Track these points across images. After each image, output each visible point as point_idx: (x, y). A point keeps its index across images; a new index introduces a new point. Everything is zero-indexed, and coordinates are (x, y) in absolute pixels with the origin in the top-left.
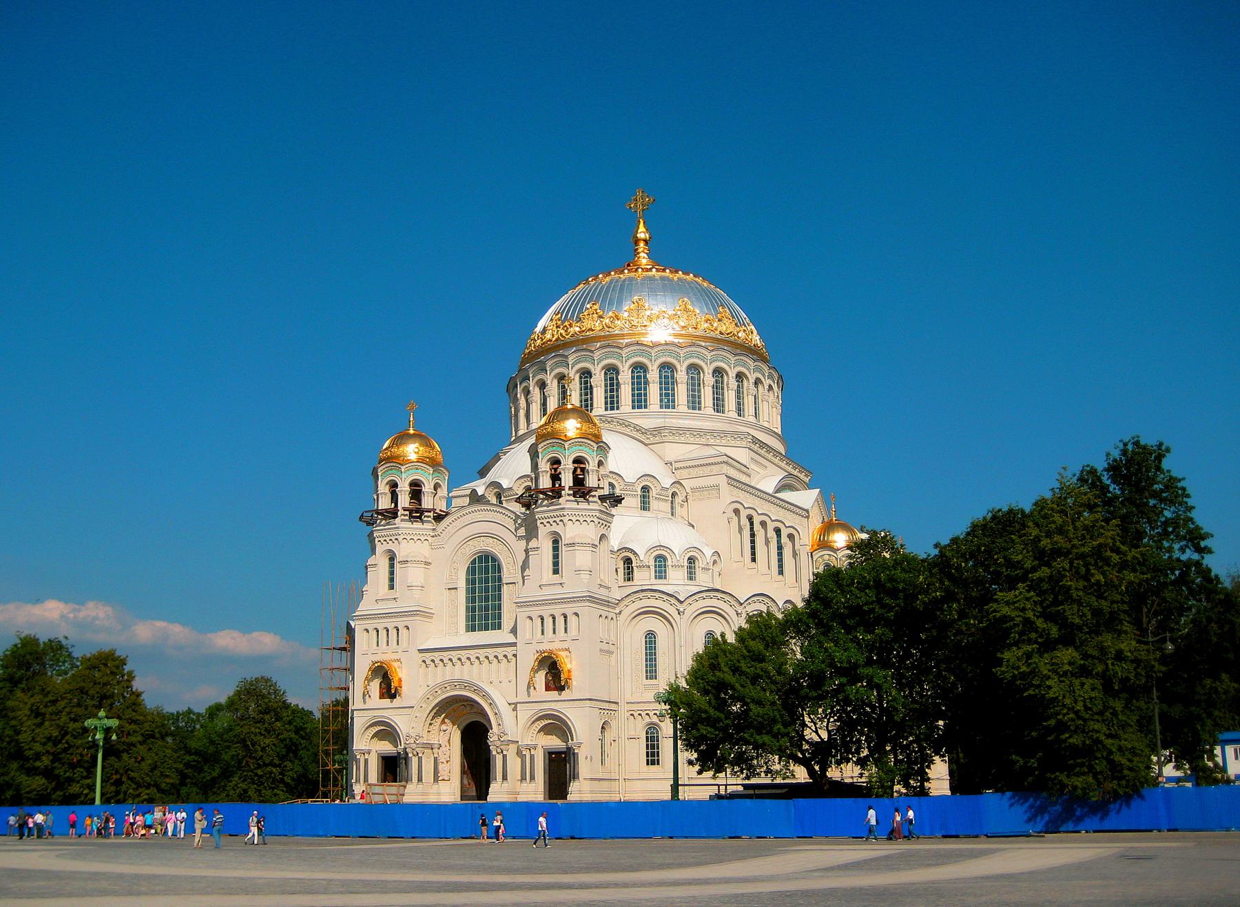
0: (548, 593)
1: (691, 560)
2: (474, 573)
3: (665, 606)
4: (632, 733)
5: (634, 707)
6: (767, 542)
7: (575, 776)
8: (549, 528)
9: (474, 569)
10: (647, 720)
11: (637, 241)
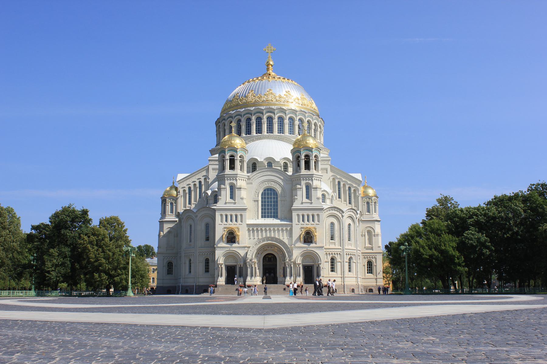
1: (332, 196)
2: (265, 195)
3: (338, 213)
4: (326, 260)
5: (327, 250)
6: (344, 190)
7: (318, 275)
8: (305, 182)
9: (265, 193)
10: (331, 255)
11: (268, 65)
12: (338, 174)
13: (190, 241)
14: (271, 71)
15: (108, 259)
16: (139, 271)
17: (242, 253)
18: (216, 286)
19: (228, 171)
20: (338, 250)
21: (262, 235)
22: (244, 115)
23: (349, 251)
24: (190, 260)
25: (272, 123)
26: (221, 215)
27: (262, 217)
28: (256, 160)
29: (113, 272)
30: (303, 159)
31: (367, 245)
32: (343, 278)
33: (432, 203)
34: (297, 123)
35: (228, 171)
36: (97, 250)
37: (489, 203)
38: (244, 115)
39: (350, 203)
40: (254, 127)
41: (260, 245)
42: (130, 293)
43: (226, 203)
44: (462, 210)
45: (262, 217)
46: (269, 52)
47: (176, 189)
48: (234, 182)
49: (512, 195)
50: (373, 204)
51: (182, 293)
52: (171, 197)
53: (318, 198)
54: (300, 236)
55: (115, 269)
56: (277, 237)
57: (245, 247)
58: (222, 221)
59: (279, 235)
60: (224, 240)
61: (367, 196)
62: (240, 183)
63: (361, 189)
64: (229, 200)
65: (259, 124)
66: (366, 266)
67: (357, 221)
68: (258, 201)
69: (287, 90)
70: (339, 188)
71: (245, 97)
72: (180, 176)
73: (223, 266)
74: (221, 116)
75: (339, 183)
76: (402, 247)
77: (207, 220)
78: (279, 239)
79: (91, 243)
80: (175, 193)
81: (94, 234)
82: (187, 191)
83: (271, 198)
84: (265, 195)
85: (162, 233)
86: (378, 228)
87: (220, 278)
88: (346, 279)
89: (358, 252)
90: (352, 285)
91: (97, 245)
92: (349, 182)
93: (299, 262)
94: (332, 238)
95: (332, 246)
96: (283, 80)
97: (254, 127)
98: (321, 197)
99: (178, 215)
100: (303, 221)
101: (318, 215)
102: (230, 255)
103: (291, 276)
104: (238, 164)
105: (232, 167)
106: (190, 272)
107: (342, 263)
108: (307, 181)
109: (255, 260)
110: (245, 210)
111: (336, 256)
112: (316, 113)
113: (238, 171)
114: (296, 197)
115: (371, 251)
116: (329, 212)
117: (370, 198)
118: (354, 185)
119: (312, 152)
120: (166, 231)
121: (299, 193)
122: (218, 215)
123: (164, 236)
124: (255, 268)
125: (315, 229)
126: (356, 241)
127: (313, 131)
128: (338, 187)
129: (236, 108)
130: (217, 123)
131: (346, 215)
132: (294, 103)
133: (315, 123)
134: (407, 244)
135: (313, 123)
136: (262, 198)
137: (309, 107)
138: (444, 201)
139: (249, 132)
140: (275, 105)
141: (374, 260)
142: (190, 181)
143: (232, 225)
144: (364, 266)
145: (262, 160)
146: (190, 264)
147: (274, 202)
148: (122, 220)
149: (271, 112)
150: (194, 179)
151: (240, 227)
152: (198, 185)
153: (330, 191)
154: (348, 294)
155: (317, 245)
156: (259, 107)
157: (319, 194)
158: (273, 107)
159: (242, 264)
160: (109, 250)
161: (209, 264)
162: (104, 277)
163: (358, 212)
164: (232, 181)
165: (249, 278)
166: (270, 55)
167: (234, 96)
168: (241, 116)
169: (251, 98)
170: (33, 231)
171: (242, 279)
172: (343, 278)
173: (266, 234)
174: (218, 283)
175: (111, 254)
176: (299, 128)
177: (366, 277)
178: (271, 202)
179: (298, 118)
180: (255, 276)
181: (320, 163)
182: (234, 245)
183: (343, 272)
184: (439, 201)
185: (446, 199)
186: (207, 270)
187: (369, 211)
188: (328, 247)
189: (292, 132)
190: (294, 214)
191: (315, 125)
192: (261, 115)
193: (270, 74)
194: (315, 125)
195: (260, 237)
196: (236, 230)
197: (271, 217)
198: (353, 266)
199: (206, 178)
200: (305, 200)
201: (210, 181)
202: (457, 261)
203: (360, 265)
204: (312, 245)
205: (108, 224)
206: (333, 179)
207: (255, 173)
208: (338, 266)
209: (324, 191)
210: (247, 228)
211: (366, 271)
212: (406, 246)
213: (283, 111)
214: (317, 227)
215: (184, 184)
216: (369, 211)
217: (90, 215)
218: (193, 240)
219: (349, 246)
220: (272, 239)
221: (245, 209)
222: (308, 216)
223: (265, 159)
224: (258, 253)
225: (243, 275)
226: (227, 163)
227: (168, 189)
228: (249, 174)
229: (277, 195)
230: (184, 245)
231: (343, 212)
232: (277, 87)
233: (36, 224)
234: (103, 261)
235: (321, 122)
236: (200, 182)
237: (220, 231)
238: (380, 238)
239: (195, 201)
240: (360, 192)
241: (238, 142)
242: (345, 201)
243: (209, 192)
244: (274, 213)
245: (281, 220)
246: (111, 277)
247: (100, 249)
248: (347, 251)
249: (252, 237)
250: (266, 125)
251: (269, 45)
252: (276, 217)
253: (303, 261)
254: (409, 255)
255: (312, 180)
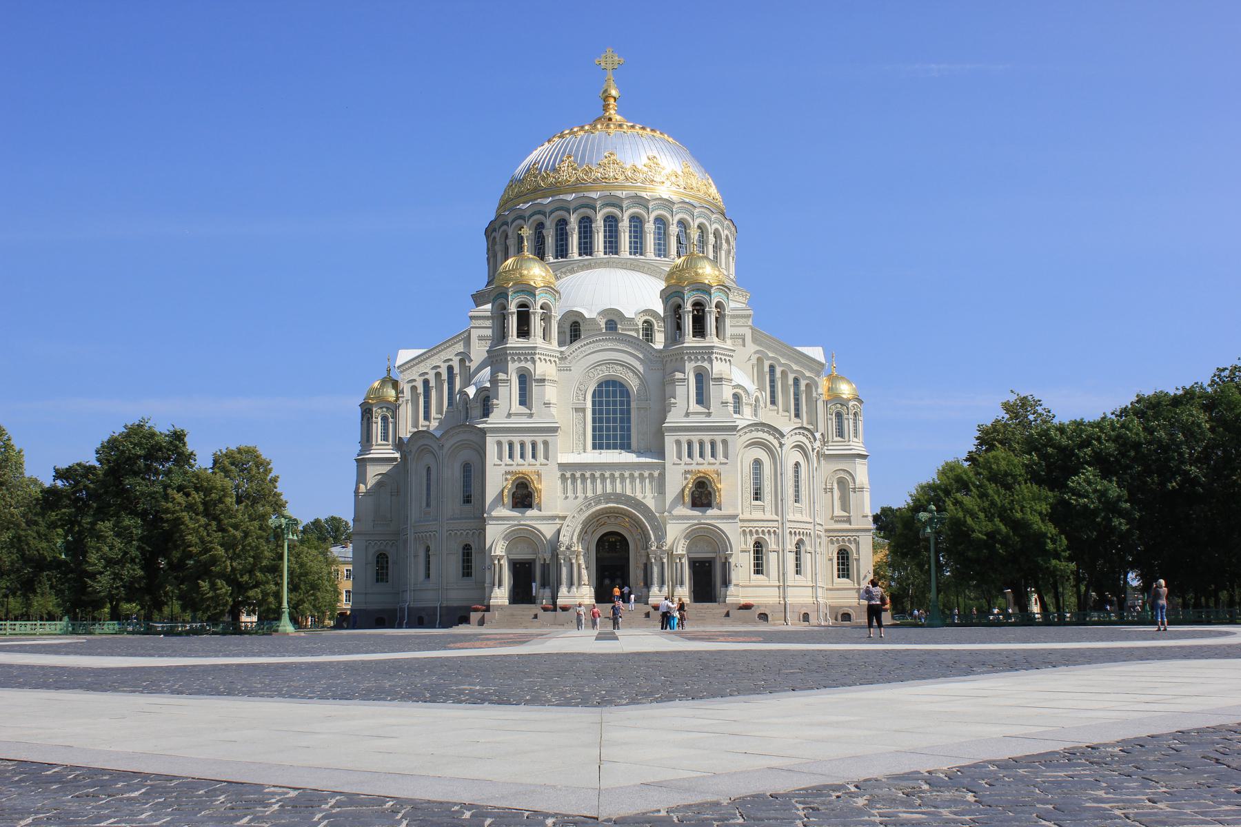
0: (694, 421)
1: (757, 400)
2: (600, 396)
3: (771, 438)
4: (743, 546)
5: (746, 524)
6: (785, 386)
7: (726, 583)
8: (693, 364)
9: (600, 393)
10: (755, 536)
11: (606, 98)
12: (769, 348)
13: (428, 505)
14: (612, 112)
15: (234, 546)
16: (306, 574)
17: (548, 530)
18: (488, 609)
19: (513, 341)
20: (770, 524)
21: (594, 490)
22: (552, 212)
23: (796, 525)
24: (428, 549)
25: (617, 231)
26: (499, 444)
27: (594, 447)
28: (580, 315)
29: (246, 578)
30: (688, 312)
31: (838, 512)
32: (783, 587)
33: (992, 412)
34: (674, 230)
35: (513, 341)
36: (206, 526)
37: (1124, 412)
38: (552, 212)
39: (797, 415)
40: (574, 240)
41: (590, 512)
42: (286, 626)
43: (509, 415)
44: (1061, 429)
45: (594, 447)
46: (610, 67)
47: (395, 384)
48: (529, 365)
49: (1180, 392)
50: (851, 416)
51: (409, 626)
52: (383, 403)
53: (725, 403)
54: (683, 490)
55: (251, 572)
56: (629, 493)
57: (553, 518)
58: (500, 458)
59: (634, 489)
60: (506, 500)
61: (836, 399)
62: (542, 368)
63: (823, 384)
64: (516, 407)
65: (585, 232)
66: (835, 561)
67: (813, 456)
68: (583, 410)
69: (650, 154)
70: (772, 381)
71: (554, 170)
72: (404, 356)
73: (505, 562)
74: (498, 216)
75: (772, 369)
76: (923, 516)
77: (466, 455)
78: (634, 499)
79: (190, 507)
80: (393, 393)
81: (197, 489)
82: (421, 390)
83: (615, 403)
84: (600, 396)
85: (362, 486)
86: (861, 473)
87: (496, 590)
88: (790, 591)
89: (818, 527)
90: (802, 606)
91: (206, 513)
92: (795, 367)
93: (680, 552)
94: (757, 496)
95: (758, 515)
96: (640, 132)
97: (574, 240)
98: (731, 399)
99: (399, 445)
100: (690, 455)
101: (725, 442)
102: (521, 537)
103: (662, 583)
104: (536, 324)
105: (524, 332)
106: (428, 576)
107: (781, 553)
108: (699, 363)
109: (578, 548)
110: (554, 430)
111: (766, 537)
112: (718, 207)
113: (536, 339)
114: (673, 400)
115: (846, 526)
116: (749, 436)
117: (844, 403)
118: (808, 374)
119: (710, 294)
120: (371, 481)
121: (680, 390)
122: (491, 443)
123: (368, 493)
124: (579, 566)
125: (719, 474)
126: (812, 502)
127: (711, 248)
128: (771, 378)
129: (532, 196)
130: (490, 231)
131: (789, 442)
132: (668, 183)
133: (716, 230)
134: (934, 508)
135: (711, 230)
136: (594, 403)
137: (701, 194)
138: (1020, 409)
139: (562, 251)
140: (622, 188)
141: (853, 547)
142: (426, 367)
143: (525, 466)
144: (831, 560)
145: (594, 315)
146: (428, 557)
147: (622, 412)
148: (265, 454)
149: (613, 205)
150: (435, 361)
151: (543, 470)
152: (445, 376)
153: (752, 387)
154: (794, 625)
155: (723, 512)
156: (586, 194)
157: (727, 393)
158: (619, 193)
159: (548, 556)
160: (236, 527)
161: (471, 558)
162: (224, 588)
163: (818, 435)
164: (523, 364)
165: (563, 590)
166: (610, 75)
167: (529, 169)
168: (544, 214)
169: (566, 174)
170: (59, 483)
171: (548, 592)
172: (783, 587)
173: (604, 487)
174: (492, 602)
175: (239, 534)
176: (679, 242)
177: (835, 586)
178: (615, 412)
179: (676, 219)
180: (579, 585)
181: (728, 321)
182: (529, 513)
183: (782, 575)
184: (1007, 407)
185: (1024, 402)
186: (467, 571)
187: (840, 433)
188: (747, 516)
189: (662, 250)
190: (670, 441)
191: (717, 234)
192: (589, 212)
193: (610, 119)
194: (717, 234)
195: (590, 494)
196: (534, 477)
197: (615, 448)
198: (807, 559)
199: (464, 358)
200: (694, 407)
201: (473, 366)
202: (1050, 546)
203: (822, 559)
204: (710, 512)
205: (233, 464)
206: (759, 359)
207: (576, 345)
208: (772, 560)
209: (738, 386)
210: (559, 474)
211: (836, 573)
212: (931, 511)
213: (641, 202)
214: (722, 469)
215: (414, 374)
216: (840, 433)
217: (191, 445)
218: (433, 503)
219: (796, 515)
220: (618, 498)
221: (554, 430)
222: (701, 444)
223: (599, 314)
224: (584, 532)
225: (551, 582)
226: (513, 322)
227: (376, 384)
228: (563, 349)
229: (628, 396)
230: (414, 513)
231: (782, 435)
232: (628, 146)
233: (63, 465)
234: (220, 551)
235: (728, 228)
236: (450, 369)
237: (496, 480)
238: (867, 495)
239: (440, 411)
240: (820, 391)
241: (536, 273)
242: (787, 410)
243: (471, 391)
244: (622, 437)
245: (639, 453)
246: (239, 588)
247: (214, 523)
248: (792, 525)
249: (570, 494)
250: (601, 235)
251: (609, 51)
252: (626, 446)
253: (689, 550)
254: (938, 533)
255: (711, 361)
